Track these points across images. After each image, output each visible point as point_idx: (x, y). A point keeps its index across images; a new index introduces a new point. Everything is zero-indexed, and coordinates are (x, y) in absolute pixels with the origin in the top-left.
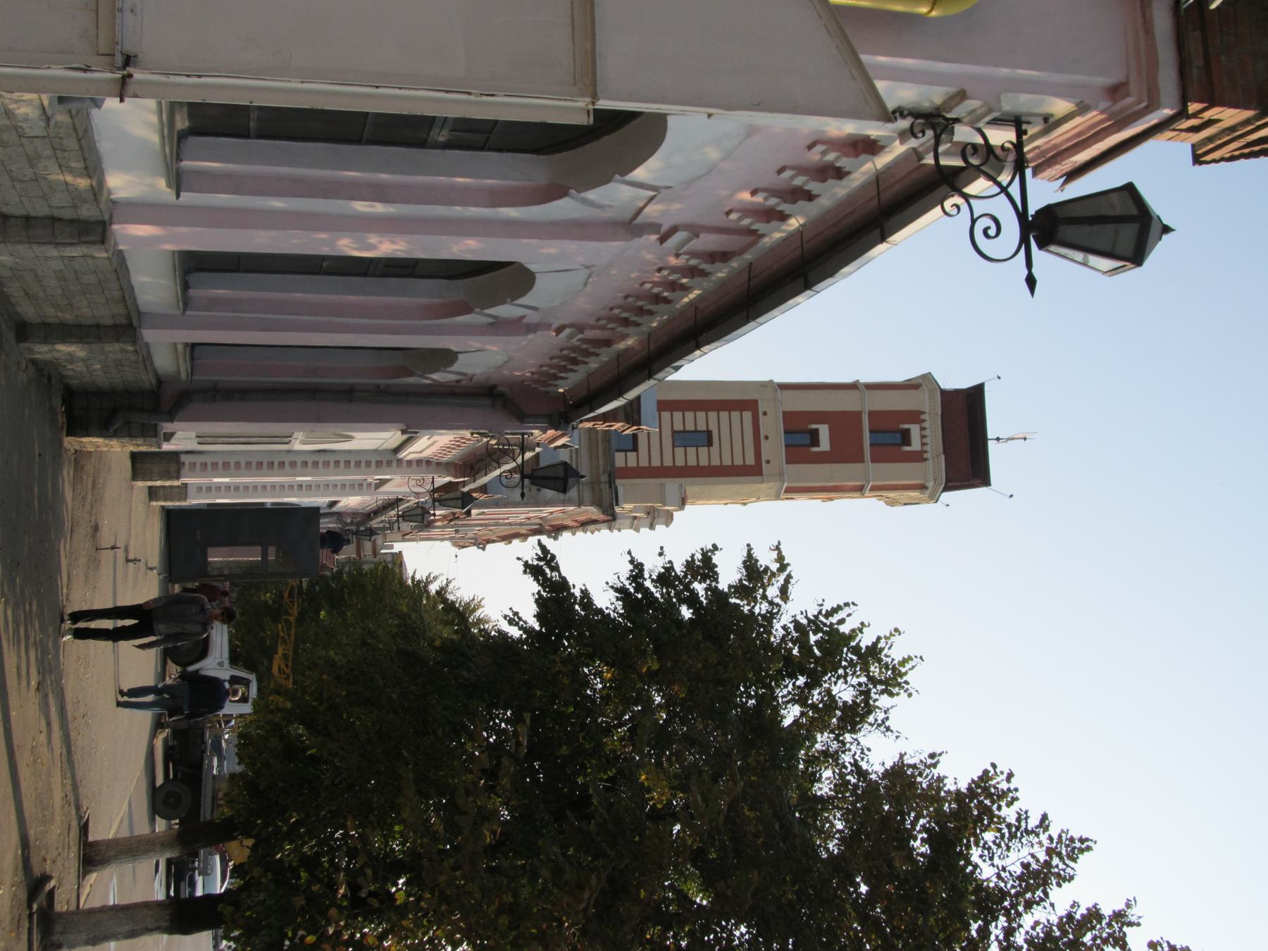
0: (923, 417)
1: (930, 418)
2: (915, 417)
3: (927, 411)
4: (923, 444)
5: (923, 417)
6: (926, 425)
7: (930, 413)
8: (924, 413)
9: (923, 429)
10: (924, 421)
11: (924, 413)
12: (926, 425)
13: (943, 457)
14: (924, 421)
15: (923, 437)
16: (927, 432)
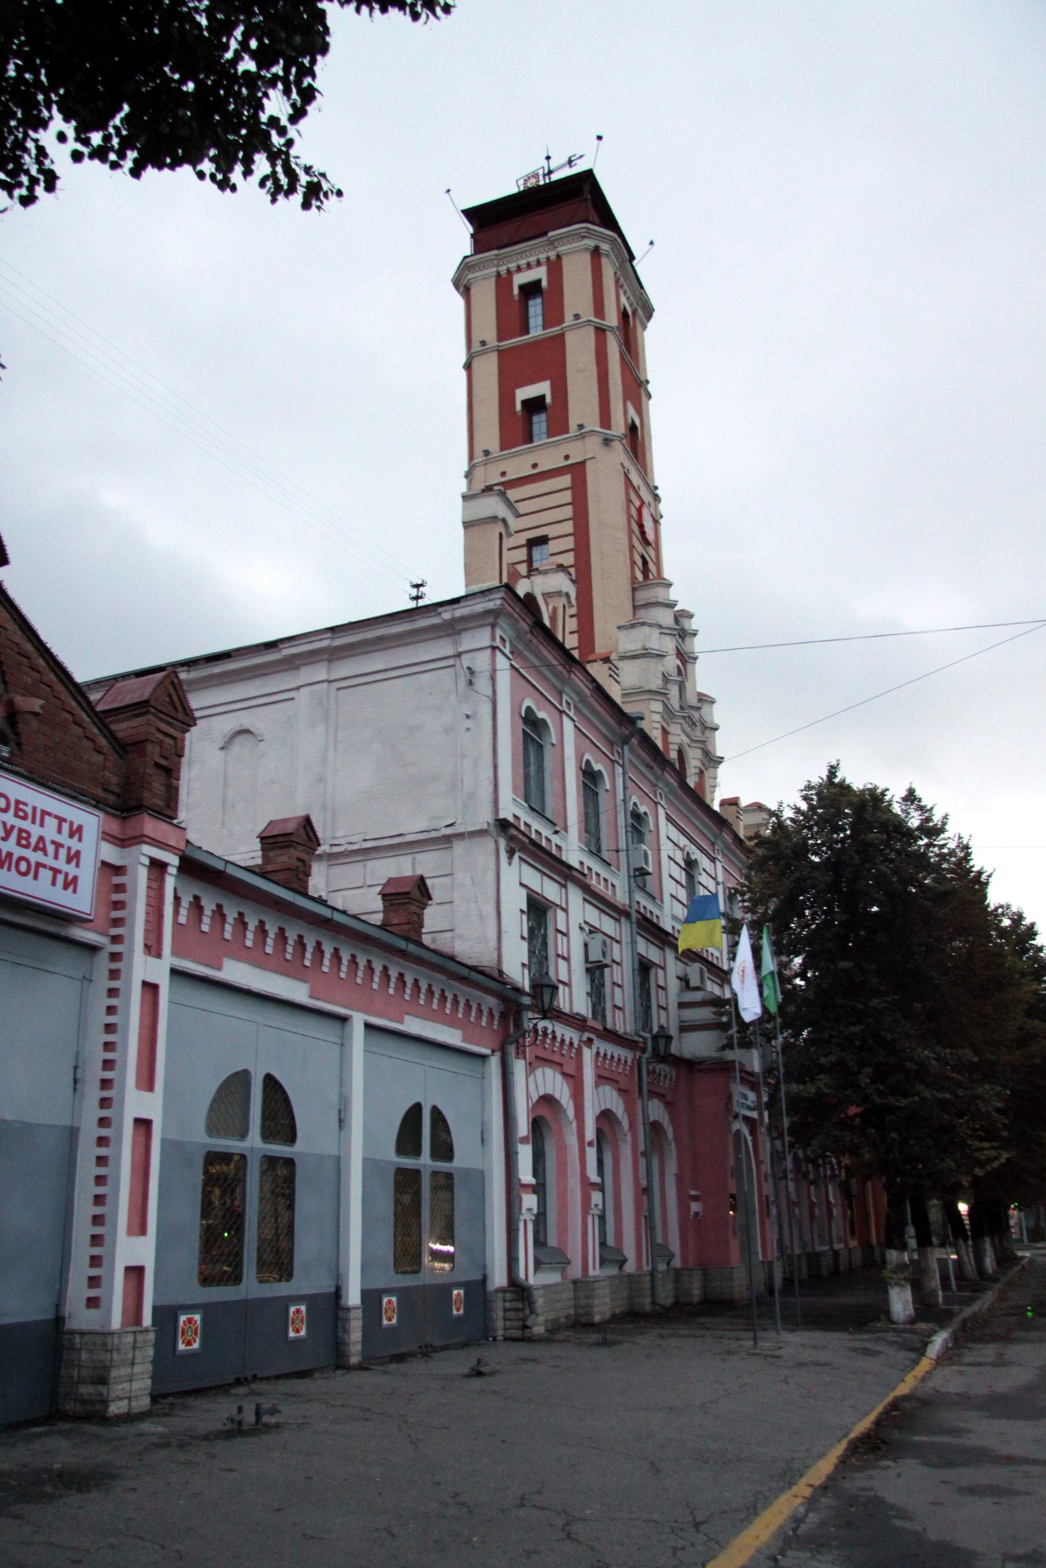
0: (503, 273)
1: (504, 264)
2: (503, 282)
3: (495, 269)
4: (539, 263)
5: (503, 273)
6: (513, 266)
7: (498, 266)
8: (498, 274)
9: (519, 269)
10: (509, 271)
11: (498, 274)
12: (513, 266)
13: (551, 234)
14: (509, 271)
15: (529, 266)
16: (523, 262)
